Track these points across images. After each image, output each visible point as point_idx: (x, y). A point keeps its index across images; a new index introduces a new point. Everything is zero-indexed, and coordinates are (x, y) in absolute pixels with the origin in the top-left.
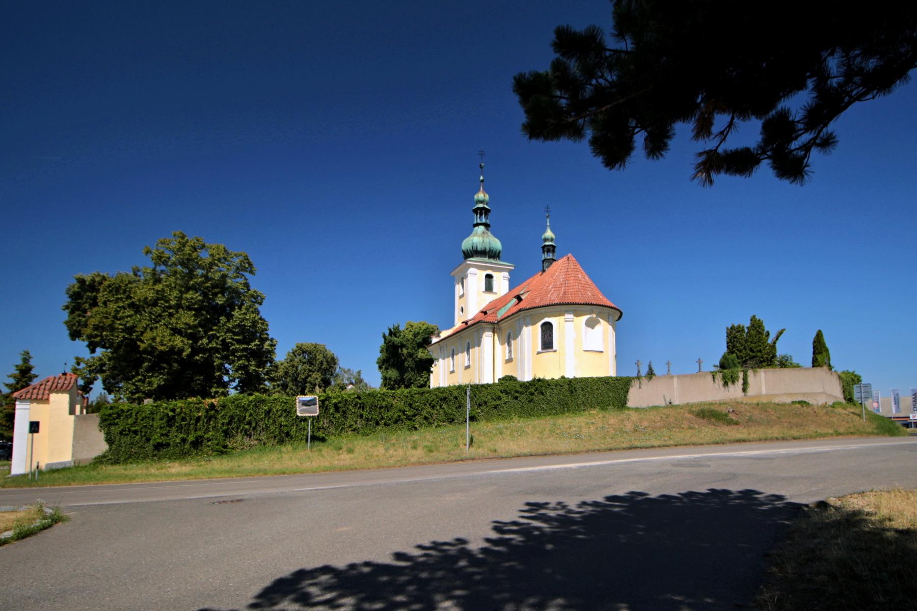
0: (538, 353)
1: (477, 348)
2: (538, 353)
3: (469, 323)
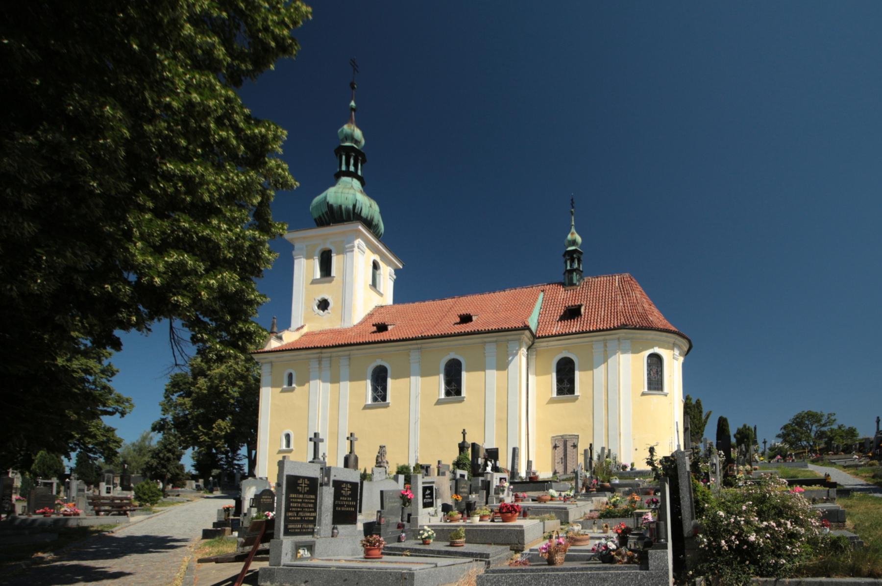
1: (492, 375)
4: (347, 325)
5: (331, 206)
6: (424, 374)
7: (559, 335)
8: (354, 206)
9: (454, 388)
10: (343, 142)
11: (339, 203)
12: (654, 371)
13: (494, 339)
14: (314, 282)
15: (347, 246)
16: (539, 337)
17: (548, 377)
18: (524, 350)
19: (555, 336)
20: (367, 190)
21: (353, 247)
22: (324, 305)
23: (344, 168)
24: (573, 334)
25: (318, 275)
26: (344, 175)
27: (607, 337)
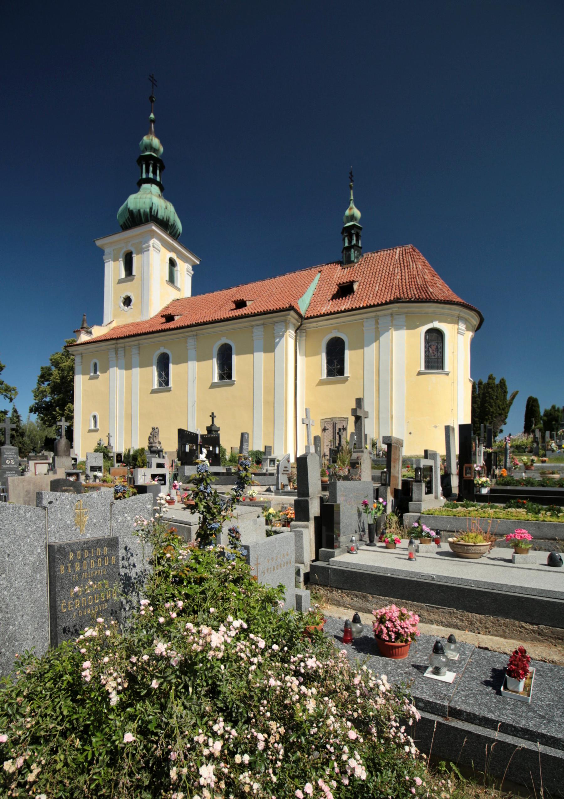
0: (420, 373)
1: (260, 357)
2: (420, 373)
3: (178, 321)
4: (146, 318)
6: (200, 359)
7: (328, 314)
8: (151, 209)
9: (226, 373)
10: (144, 152)
11: (138, 208)
12: (434, 347)
13: (261, 322)
14: (121, 281)
15: (144, 246)
16: (306, 319)
17: (318, 357)
18: (291, 333)
19: (324, 315)
20: (165, 193)
21: (149, 246)
22: (127, 301)
23: (144, 176)
24: (342, 312)
25: (123, 275)
26: (144, 183)
27: (379, 313)
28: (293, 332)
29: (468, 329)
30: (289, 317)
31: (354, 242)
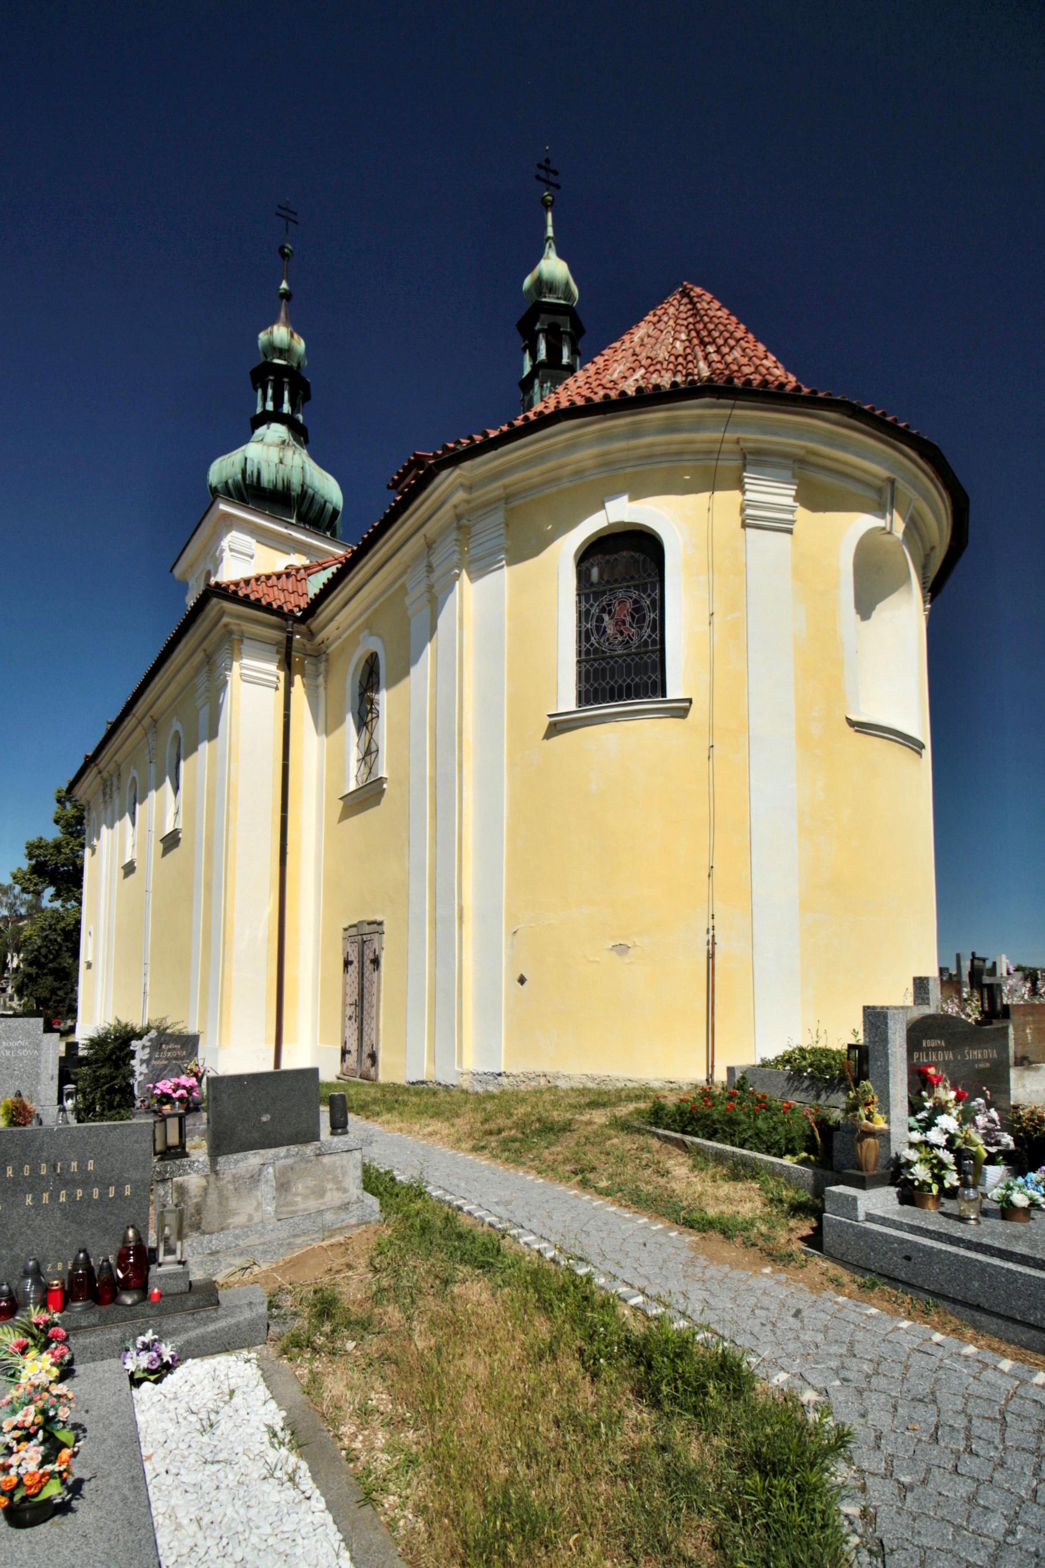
0: (557, 727)
2: (557, 727)
5: (216, 488)
8: (244, 472)
15: (218, 553)
18: (271, 669)
28: (273, 667)
29: (816, 497)
30: (225, 620)
31: (542, 355)
